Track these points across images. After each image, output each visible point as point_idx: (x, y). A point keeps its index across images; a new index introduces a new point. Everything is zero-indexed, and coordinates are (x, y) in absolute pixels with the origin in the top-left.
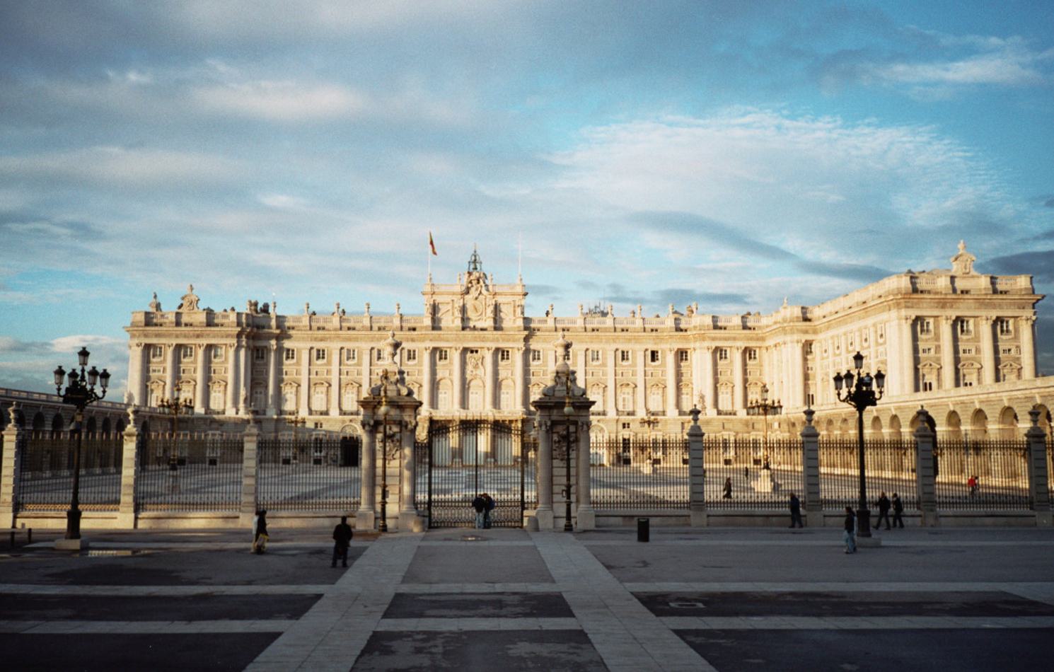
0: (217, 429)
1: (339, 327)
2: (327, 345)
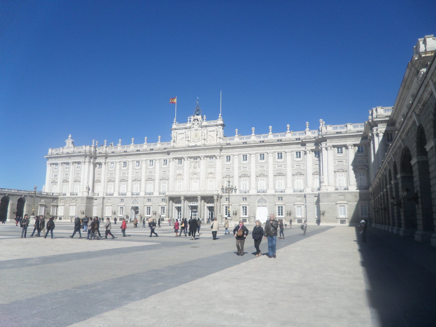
0: (74, 203)
2: (127, 160)
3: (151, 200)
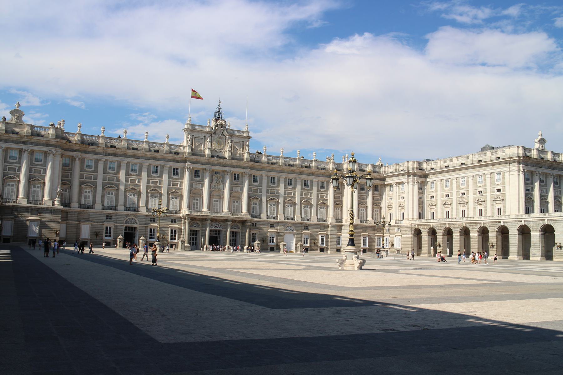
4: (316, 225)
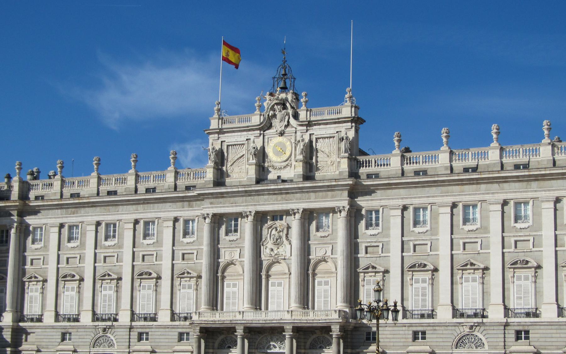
1: (96, 192)
2: (80, 219)
3: (149, 337)
4: (553, 327)
